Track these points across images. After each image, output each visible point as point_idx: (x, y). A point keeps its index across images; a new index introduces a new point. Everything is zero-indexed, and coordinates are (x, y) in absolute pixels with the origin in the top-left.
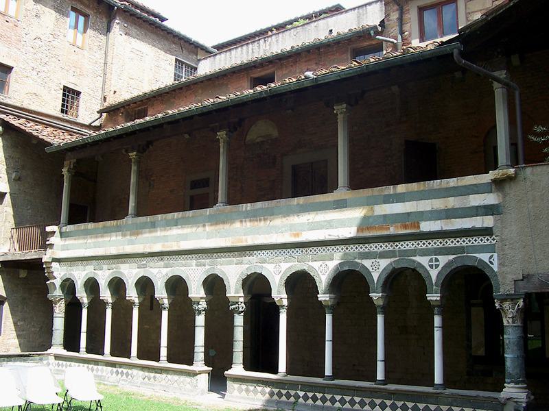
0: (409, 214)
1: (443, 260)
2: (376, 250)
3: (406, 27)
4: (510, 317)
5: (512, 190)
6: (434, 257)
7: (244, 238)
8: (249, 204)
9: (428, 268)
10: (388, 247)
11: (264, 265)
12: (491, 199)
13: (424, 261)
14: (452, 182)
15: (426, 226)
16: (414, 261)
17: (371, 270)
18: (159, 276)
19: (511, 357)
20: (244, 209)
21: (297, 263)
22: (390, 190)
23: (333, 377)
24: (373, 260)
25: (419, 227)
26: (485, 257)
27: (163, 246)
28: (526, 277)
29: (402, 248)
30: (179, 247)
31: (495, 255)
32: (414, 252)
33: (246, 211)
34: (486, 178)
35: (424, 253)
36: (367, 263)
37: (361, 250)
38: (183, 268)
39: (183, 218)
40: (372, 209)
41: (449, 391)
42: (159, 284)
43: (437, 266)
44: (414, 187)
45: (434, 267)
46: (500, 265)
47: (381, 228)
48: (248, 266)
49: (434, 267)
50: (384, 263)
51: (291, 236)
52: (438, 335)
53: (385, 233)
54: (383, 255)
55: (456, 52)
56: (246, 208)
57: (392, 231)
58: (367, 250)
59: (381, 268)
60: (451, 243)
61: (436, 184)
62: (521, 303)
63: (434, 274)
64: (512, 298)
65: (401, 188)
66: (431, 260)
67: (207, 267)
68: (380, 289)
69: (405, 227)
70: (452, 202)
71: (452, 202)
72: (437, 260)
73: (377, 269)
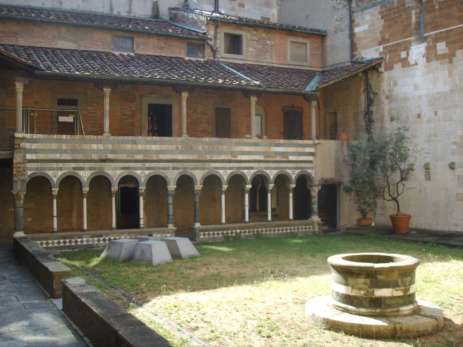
0: (285, 152)
1: (297, 171)
2: (272, 166)
3: (218, 41)
4: (315, 192)
5: (318, 147)
6: (293, 170)
7: (205, 156)
8: (207, 138)
9: (292, 175)
10: (276, 165)
11: (217, 170)
12: (312, 150)
13: (290, 171)
14: (300, 142)
15: (291, 158)
16: (286, 172)
17: (269, 174)
18: (143, 175)
19: (315, 207)
20: (204, 140)
21: (235, 170)
22: (277, 141)
23: (250, 221)
24: (271, 170)
25: (288, 158)
26: (310, 171)
27: (144, 156)
28: (322, 179)
29: (282, 166)
30: (159, 158)
31: (313, 171)
32: (286, 168)
33: (206, 141)
34: (311, 142)
35: (290, 168)
36: (268, 172)
37: (266, 166)
38: (162, 171)
39: (160, 140)
40: (270, 149)
41: (274, 222)
42: (143, 180)
43: (292, 174)
44: (287, 141)
45: (293, 174)
46: (315, 174)
47: (274, 157)
48: (208, 171)
49: (293, 174)
50: (275, 172)
51: (232, 157)
52: (291, 200)
53: (275, 159)
54: (275, 168)
55: (318, 95)
56: (206, 140)
57: (278, 159)
58: (268, 166)
59: (274, 174)
60: (299, 165)
61: (295, 141)
62: (320, 187)
63: (293, 177)
64: (318, 186)
65: (282, 141)
66: (292, 172)
67: (181, 171)
68: (273, 183)
69: (283, 157)
70: (300, 150)
71: (300, 150)
72: (294, 172)
73: (272, 174)
